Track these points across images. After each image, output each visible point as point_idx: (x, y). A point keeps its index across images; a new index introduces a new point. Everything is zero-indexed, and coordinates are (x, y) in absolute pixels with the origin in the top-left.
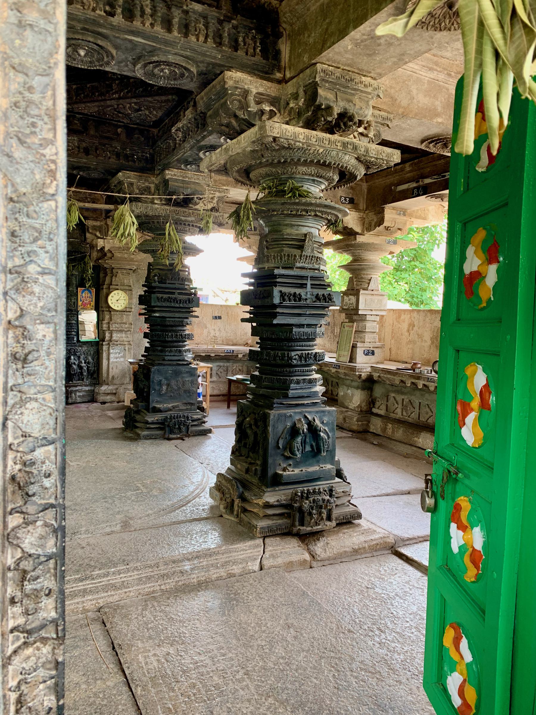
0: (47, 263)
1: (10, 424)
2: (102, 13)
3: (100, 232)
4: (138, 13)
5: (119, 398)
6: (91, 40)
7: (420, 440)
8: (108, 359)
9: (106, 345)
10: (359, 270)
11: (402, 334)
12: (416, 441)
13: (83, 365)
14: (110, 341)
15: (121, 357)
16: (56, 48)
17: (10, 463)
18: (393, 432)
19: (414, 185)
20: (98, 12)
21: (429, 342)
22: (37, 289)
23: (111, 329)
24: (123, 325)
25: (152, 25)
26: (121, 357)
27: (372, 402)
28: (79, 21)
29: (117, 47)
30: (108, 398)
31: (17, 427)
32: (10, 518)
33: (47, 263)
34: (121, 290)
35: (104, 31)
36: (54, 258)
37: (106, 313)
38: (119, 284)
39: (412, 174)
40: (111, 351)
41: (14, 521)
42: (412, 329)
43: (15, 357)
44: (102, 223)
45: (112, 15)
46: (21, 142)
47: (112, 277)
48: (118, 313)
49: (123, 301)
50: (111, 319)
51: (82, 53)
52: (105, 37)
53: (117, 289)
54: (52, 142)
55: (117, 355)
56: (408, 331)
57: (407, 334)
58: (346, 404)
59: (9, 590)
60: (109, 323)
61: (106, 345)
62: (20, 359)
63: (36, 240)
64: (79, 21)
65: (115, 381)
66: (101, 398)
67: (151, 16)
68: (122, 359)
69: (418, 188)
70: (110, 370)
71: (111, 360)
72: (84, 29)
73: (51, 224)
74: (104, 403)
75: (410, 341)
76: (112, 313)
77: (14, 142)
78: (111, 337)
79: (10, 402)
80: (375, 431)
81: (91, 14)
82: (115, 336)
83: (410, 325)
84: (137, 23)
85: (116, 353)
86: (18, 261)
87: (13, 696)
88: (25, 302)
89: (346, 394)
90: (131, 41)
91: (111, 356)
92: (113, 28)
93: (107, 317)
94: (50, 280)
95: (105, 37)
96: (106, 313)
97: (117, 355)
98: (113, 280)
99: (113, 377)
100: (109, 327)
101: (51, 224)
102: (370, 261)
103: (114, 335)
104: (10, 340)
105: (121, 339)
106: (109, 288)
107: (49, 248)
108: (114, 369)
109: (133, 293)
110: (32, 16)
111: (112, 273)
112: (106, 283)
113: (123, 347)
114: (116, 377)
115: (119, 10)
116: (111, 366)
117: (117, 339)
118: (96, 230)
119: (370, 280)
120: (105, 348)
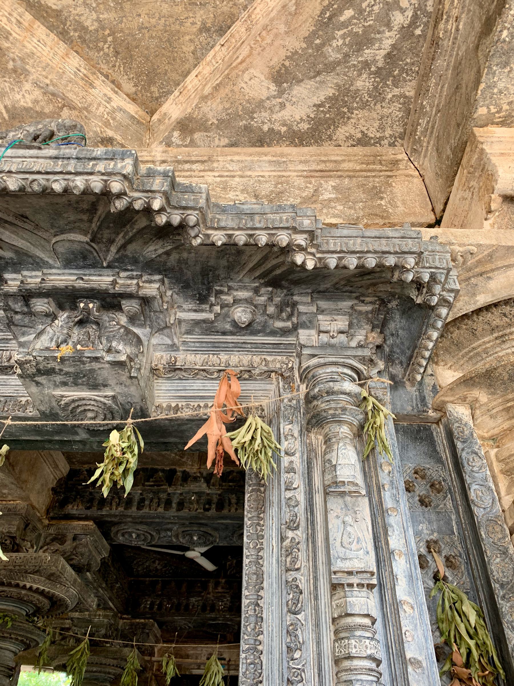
2: (202, 511)
4: (226, 505)
6: (195, 529)
20: (199, 511)
25: (236, 509)
28: (187, 519)
29: (216, 529)
35: (203, 521)
45: (208, 510)
51: (195, 538)
52: (206, 525)
64: (187, 519)
67: (237, 504)
72: (190, 523)
81: (193, 513)
84: (225, 512)
90: (222, 524)
92: (209, 518)
95: (206, 525)
115: (214, 506)
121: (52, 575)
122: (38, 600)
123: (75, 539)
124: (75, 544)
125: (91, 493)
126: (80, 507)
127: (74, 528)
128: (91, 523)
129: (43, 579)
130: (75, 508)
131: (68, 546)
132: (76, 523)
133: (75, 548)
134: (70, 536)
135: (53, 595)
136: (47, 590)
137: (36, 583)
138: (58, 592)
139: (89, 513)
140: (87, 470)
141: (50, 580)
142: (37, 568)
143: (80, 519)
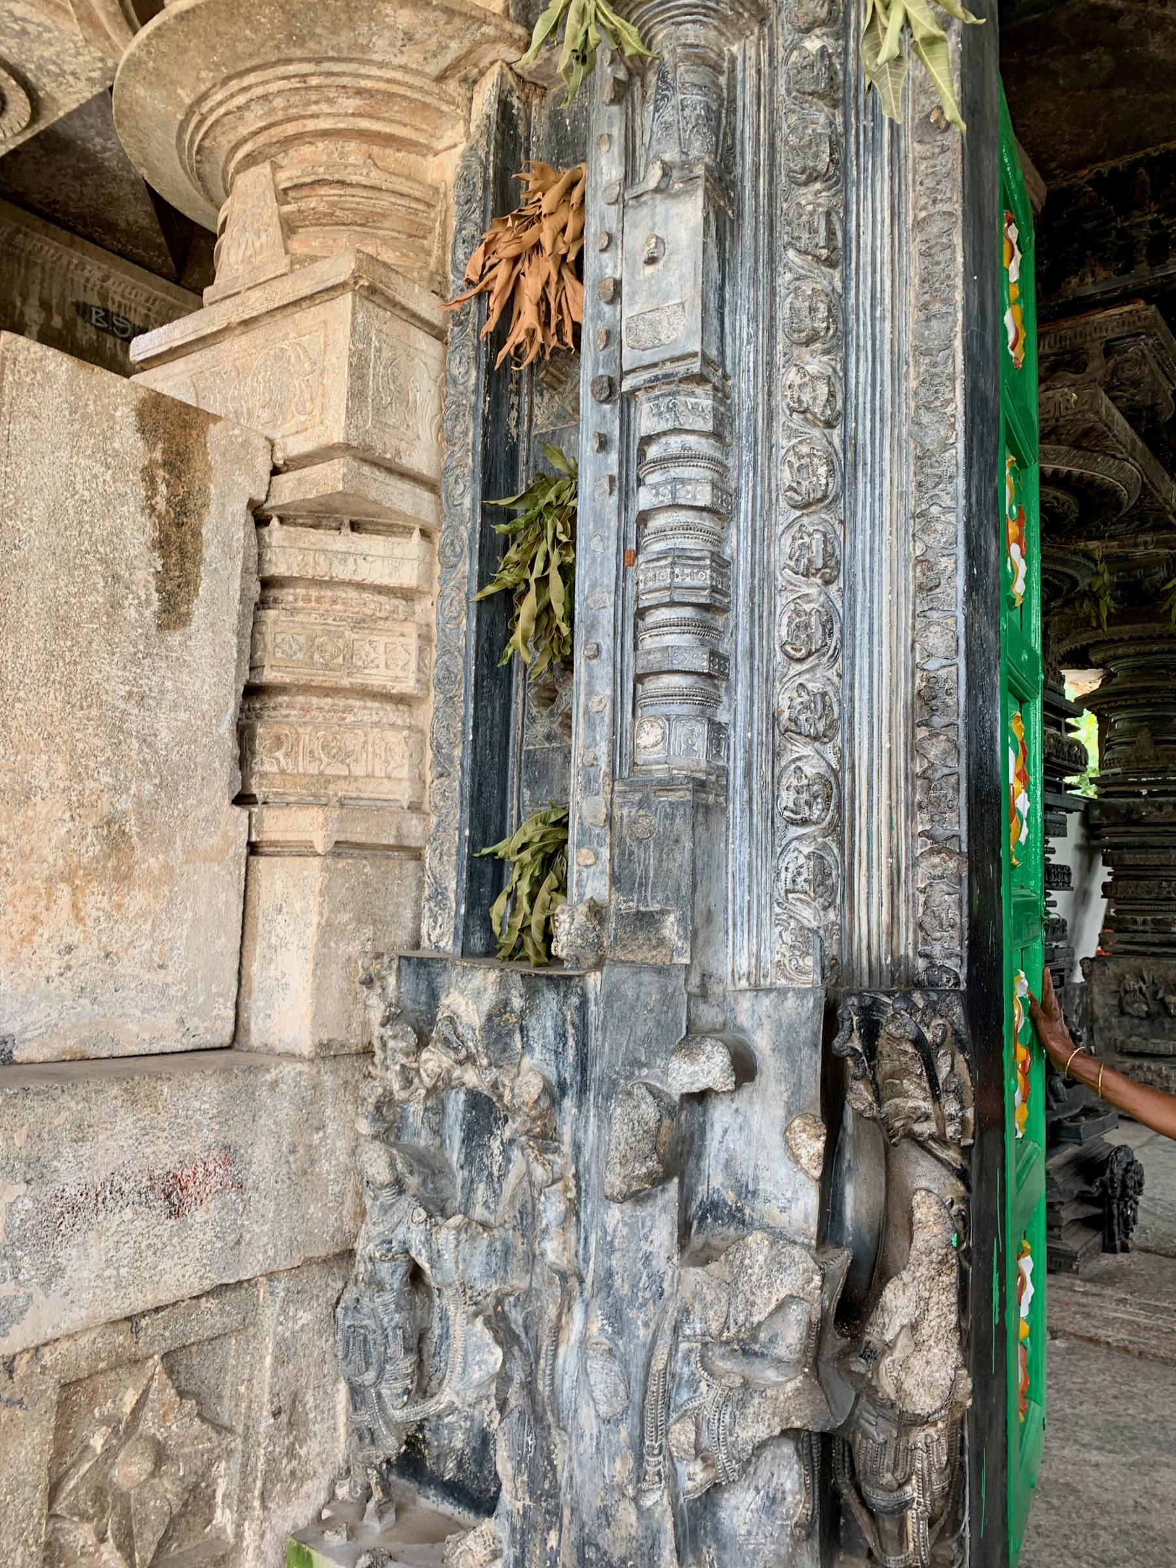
0: (947, 502)
1: (917, 646)
16: (955, 322)
17: (918, 681)
22: (939, 527)
31: (923, 649)
32: (918, 730)
33: (947, 502)
36: (955, 498)
41: (922, 733)
43: (921, 588)
46: (928, 409)
54: (952, 400)
59: (918, 797)
62: (926, 589)
63: (937, 484)
73: (953, 469)
77: (922, 412)
79: (918, 627)
86: (924, 507)
87: (922, 898)
88: (929, 539)
94: (951, 517)
101: (953, 469)
104: (918, 574)
107: (950, 490)
110: (936, 307)
121: (1086, 433)
122: (1055, 498)
123: (1108, 352)
124: (1112, 363)
125: (1122, 233)
126: (1102, 274)
127: (1099, 328)
128: (1140, 304)
129: (1064, 448)
130: (1090, 280)
131: (1097, 367)
132: (1100, 316)
133: (1114, 373)
134: (1096, 348)
135: (1091, 482)
136: (1076, 471)
137: (1050, 461)
138: (1102, 471)
139: (1129, 281)
140: (1090, 182)
141: (1079, 448)
142: (1052, 423)
143: (1107, 304)
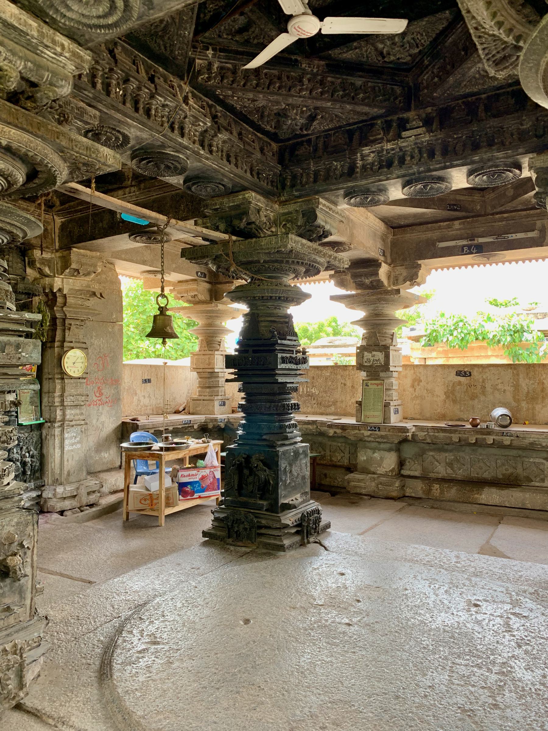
3: (49, 267)
5: (80, 501)
7: (483, 496)
8: (62, 447)
9: (59, 427)
10: (380, 325)
11: (404, 390)
12: (477, 498)
13: (28, 459)
14: (63, 420)
15: (78, 443)
18: (442, 492)
19: (465, 242)
21: (443, 397)
23: (65, 404)
24: (80, 398)
26: (78, 443)
27: (401, 464)
30: (67, 504)
34: (79, 348)
37: (57, 381)
38: (74, 340)
39: (458, 232)
40: (66, 435)
42: (418, 385)
44: (53, 256)
47: (64, 331)
48: (72, 381)
49: (81, 365)
50: (63, 390)
53: (73, 348)
55: (73, 441)
56: (413, 386)
57: (411, 390)
58: (372, 469)
60: (62, 396)
61: (59, 427)
65: (72, 479)
66: (60, 506)
68: (79, 446)
69: (469, 247)
70: (66, 463)
71: (67, 448)
74: (62, 513)
75: (416, 397)
76: (66, 381)
78: (64, 415)
80: (413, 495)
82: (70, 413)
83: (414, 380)
85: (71, 438)
89: (370, 460)
91: (67, 442)
93: (58, 387)
96: (57, 381)
97: (73, 441)
98: (67, 334)
99: (69, 474)
100: (62, 401)
102: (386, 315)
103: (68, 412)
105: (77, 418)
106: (62, 347)
108: (70, 461)
109: (90, 351)
111: (64, 325)
112: (57, 339)
113: (79, 427)
114: (72, 472)
116: (66, 457)
117: (72, 417)
118: (45, 265)
119: (393, 335)
120: (57, 431)
